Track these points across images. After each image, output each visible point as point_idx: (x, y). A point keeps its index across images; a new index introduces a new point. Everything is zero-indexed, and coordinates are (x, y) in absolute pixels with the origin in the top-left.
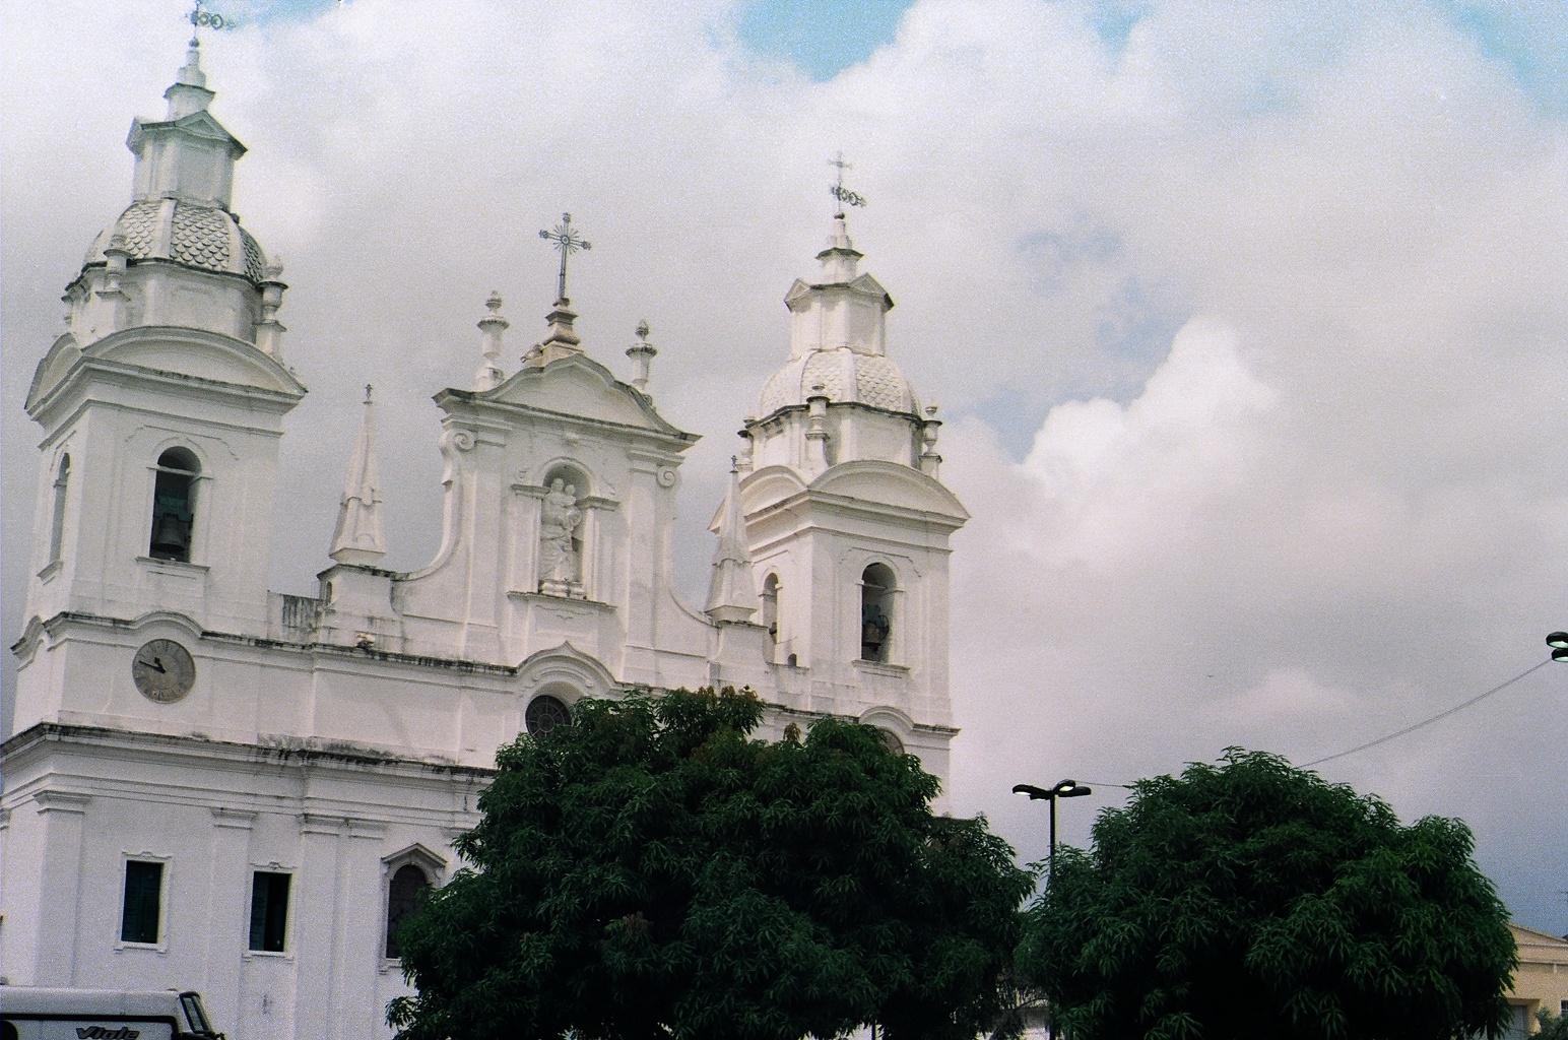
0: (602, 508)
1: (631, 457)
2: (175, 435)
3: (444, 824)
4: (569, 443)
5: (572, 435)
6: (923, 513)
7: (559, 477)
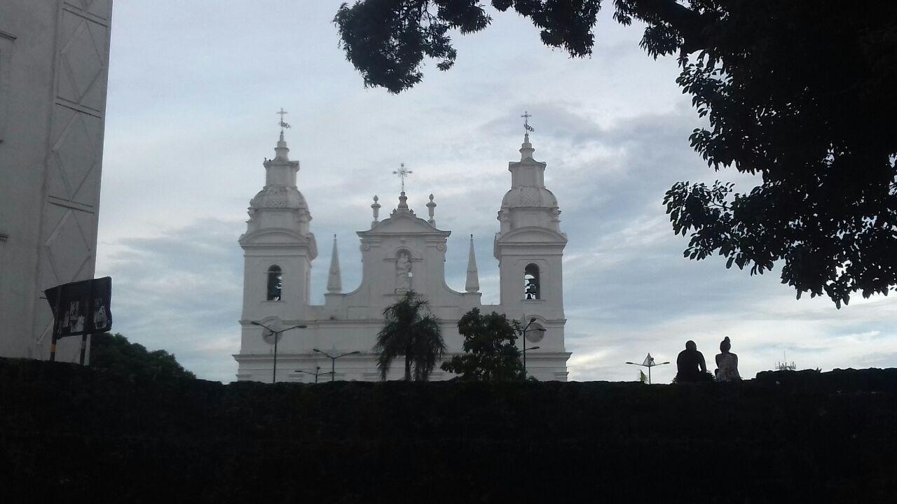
1: (427, 242)
4: (403, 242)
5: (403, 239)
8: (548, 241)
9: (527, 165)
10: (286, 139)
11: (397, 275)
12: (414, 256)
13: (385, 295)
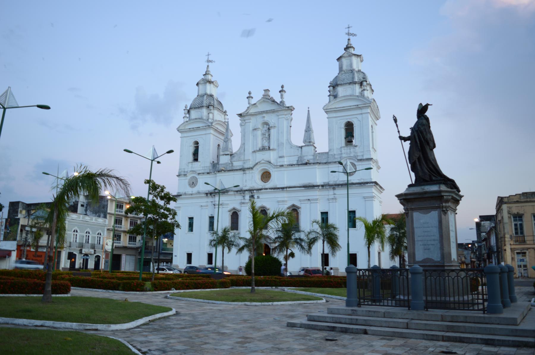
1: (278, 116)
5: (264, 115)
10: (210, 69)
12: (271, 125)
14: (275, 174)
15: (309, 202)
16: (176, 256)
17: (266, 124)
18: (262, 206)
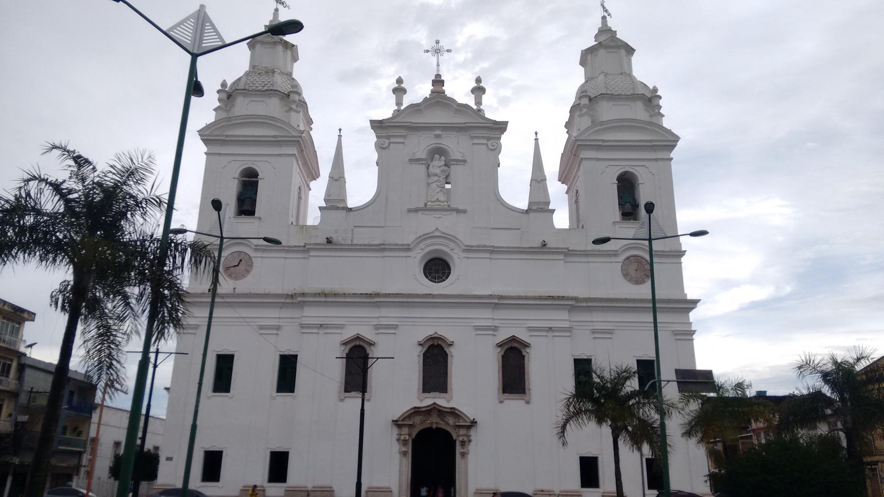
0: (457, 164)
1: (472, 138)
2: (246, 162)
3: (375, 323)
5: (439, 132)
6: (650, 141)
7: (437, 154)
8: (648, 138)
9: (611, 47)
11: (429, 184)
12: (455, 155)
13: (409, 211)
14: (459, 264)
15: (550, 334)
16: (169, 459)
17: (439, 152)
18: (436, 336)
